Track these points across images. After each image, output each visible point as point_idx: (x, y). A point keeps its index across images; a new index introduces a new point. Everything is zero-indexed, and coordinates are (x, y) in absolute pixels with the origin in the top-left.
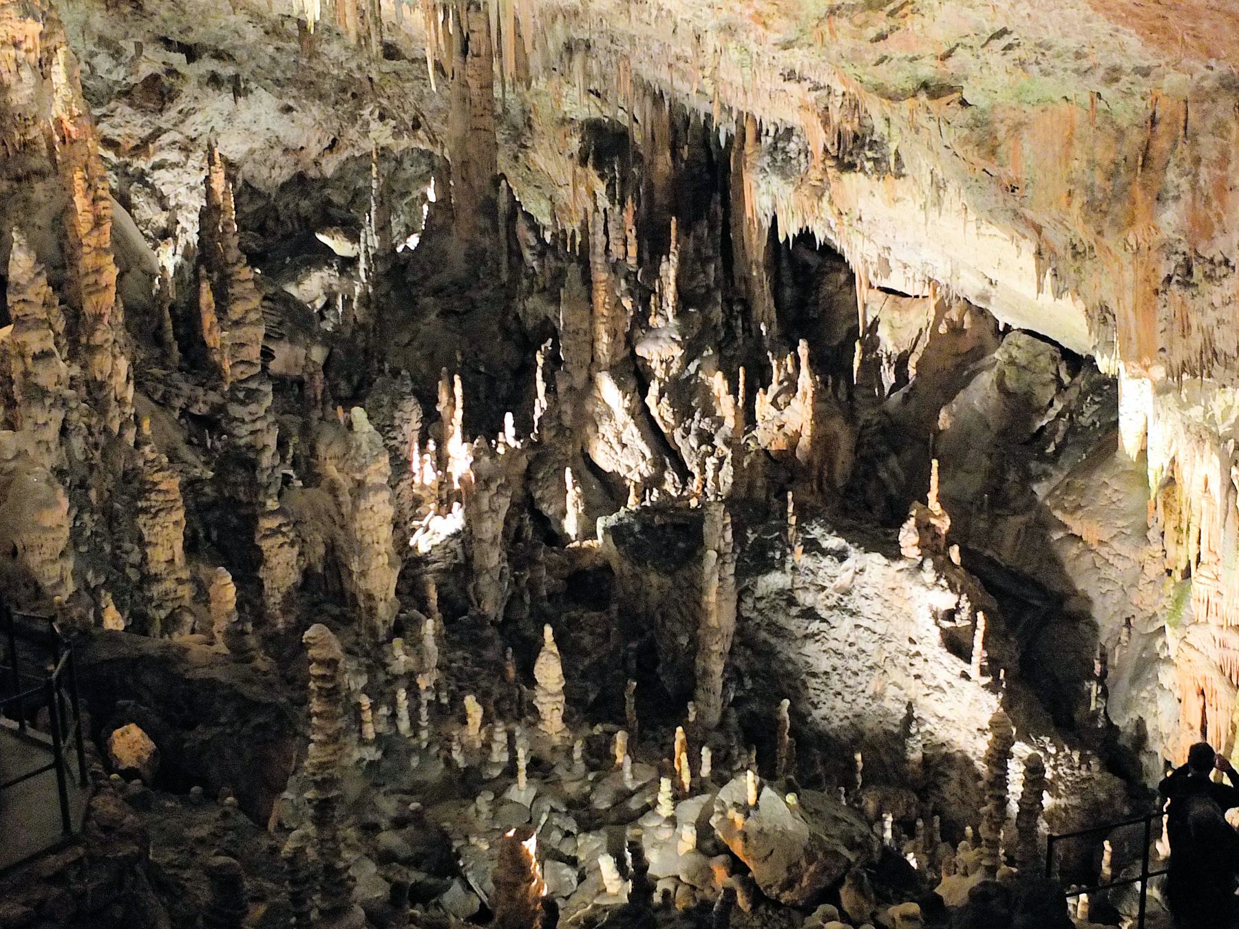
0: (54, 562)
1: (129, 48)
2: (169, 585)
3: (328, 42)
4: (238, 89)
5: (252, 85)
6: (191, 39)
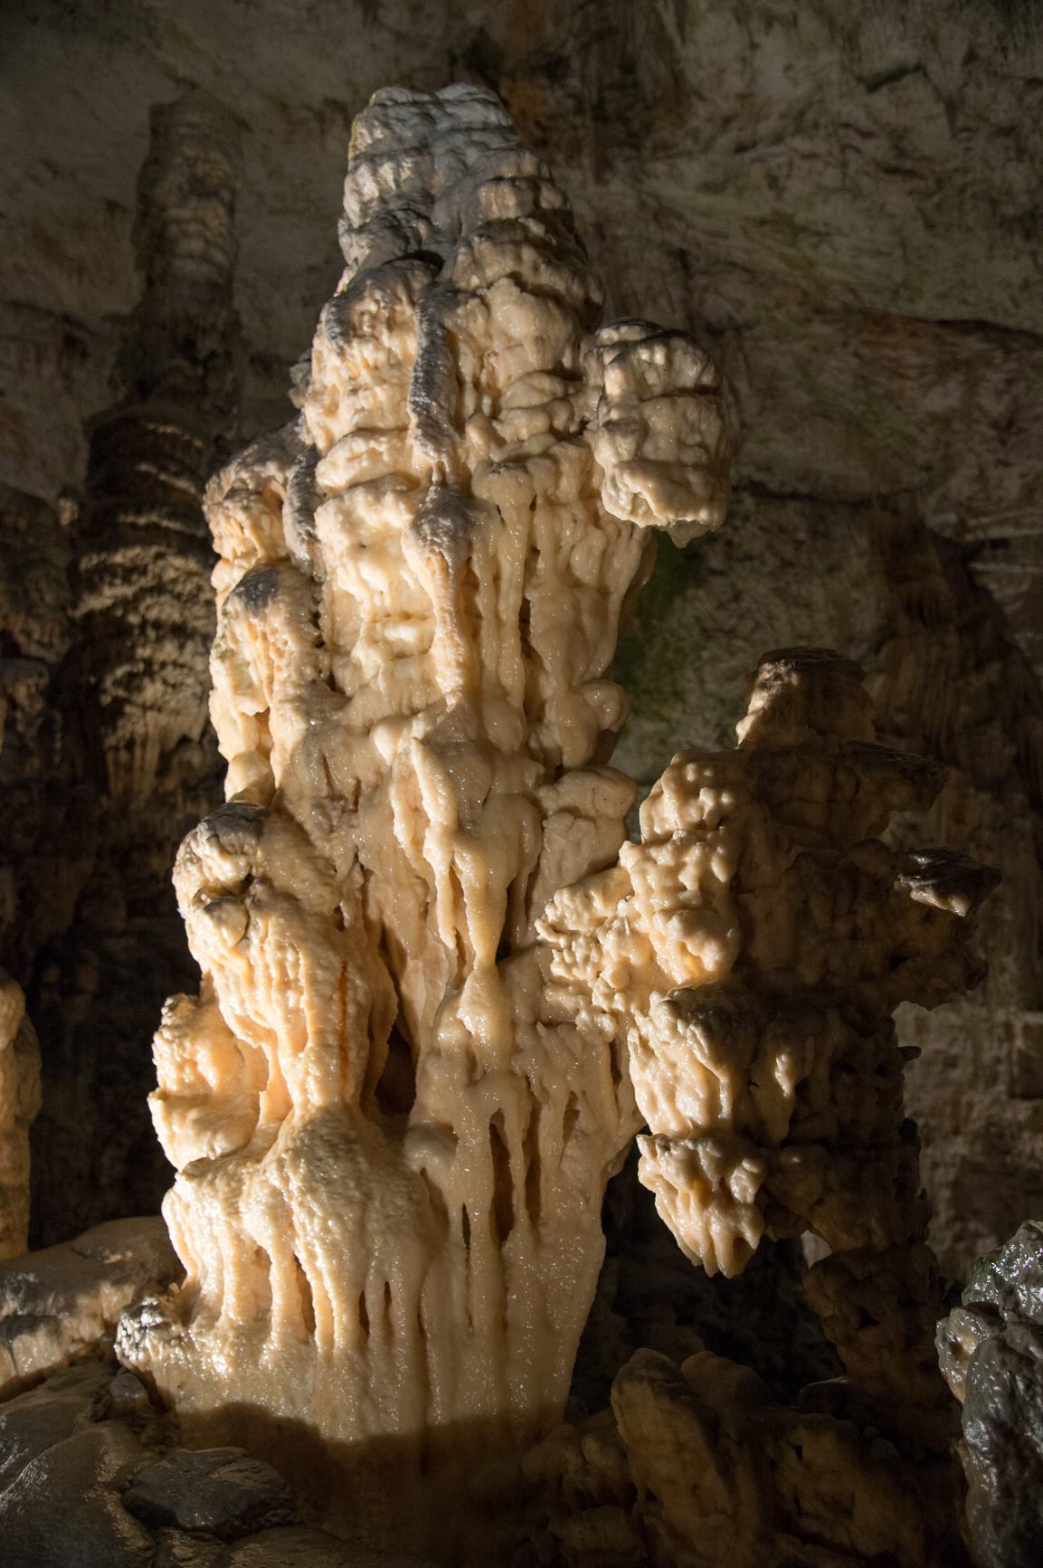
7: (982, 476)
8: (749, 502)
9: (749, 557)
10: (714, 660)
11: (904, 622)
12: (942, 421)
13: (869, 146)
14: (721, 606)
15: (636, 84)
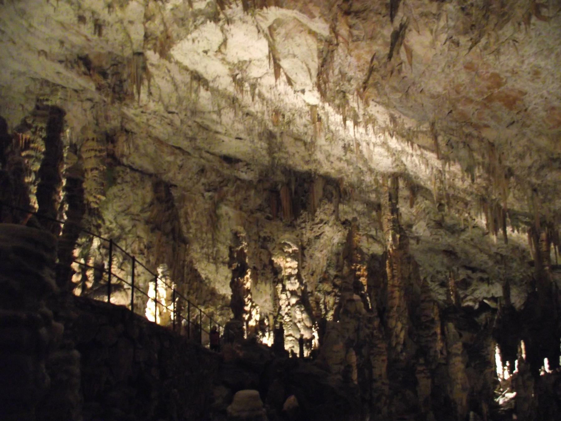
0: (336, 364)
1: (455, 268)
2: (379, 384)
3: (513, 262)
4: (488, 281)
5: (494, 281)
6: (473, 265)
7: (175, 174)
8: (128, 170)
9: (127, 182)
10: (116, 202)
11: (156, 202)
12: (169, 163)
13: (166, 120)
14: (119, 191)
15: (122, 87)
